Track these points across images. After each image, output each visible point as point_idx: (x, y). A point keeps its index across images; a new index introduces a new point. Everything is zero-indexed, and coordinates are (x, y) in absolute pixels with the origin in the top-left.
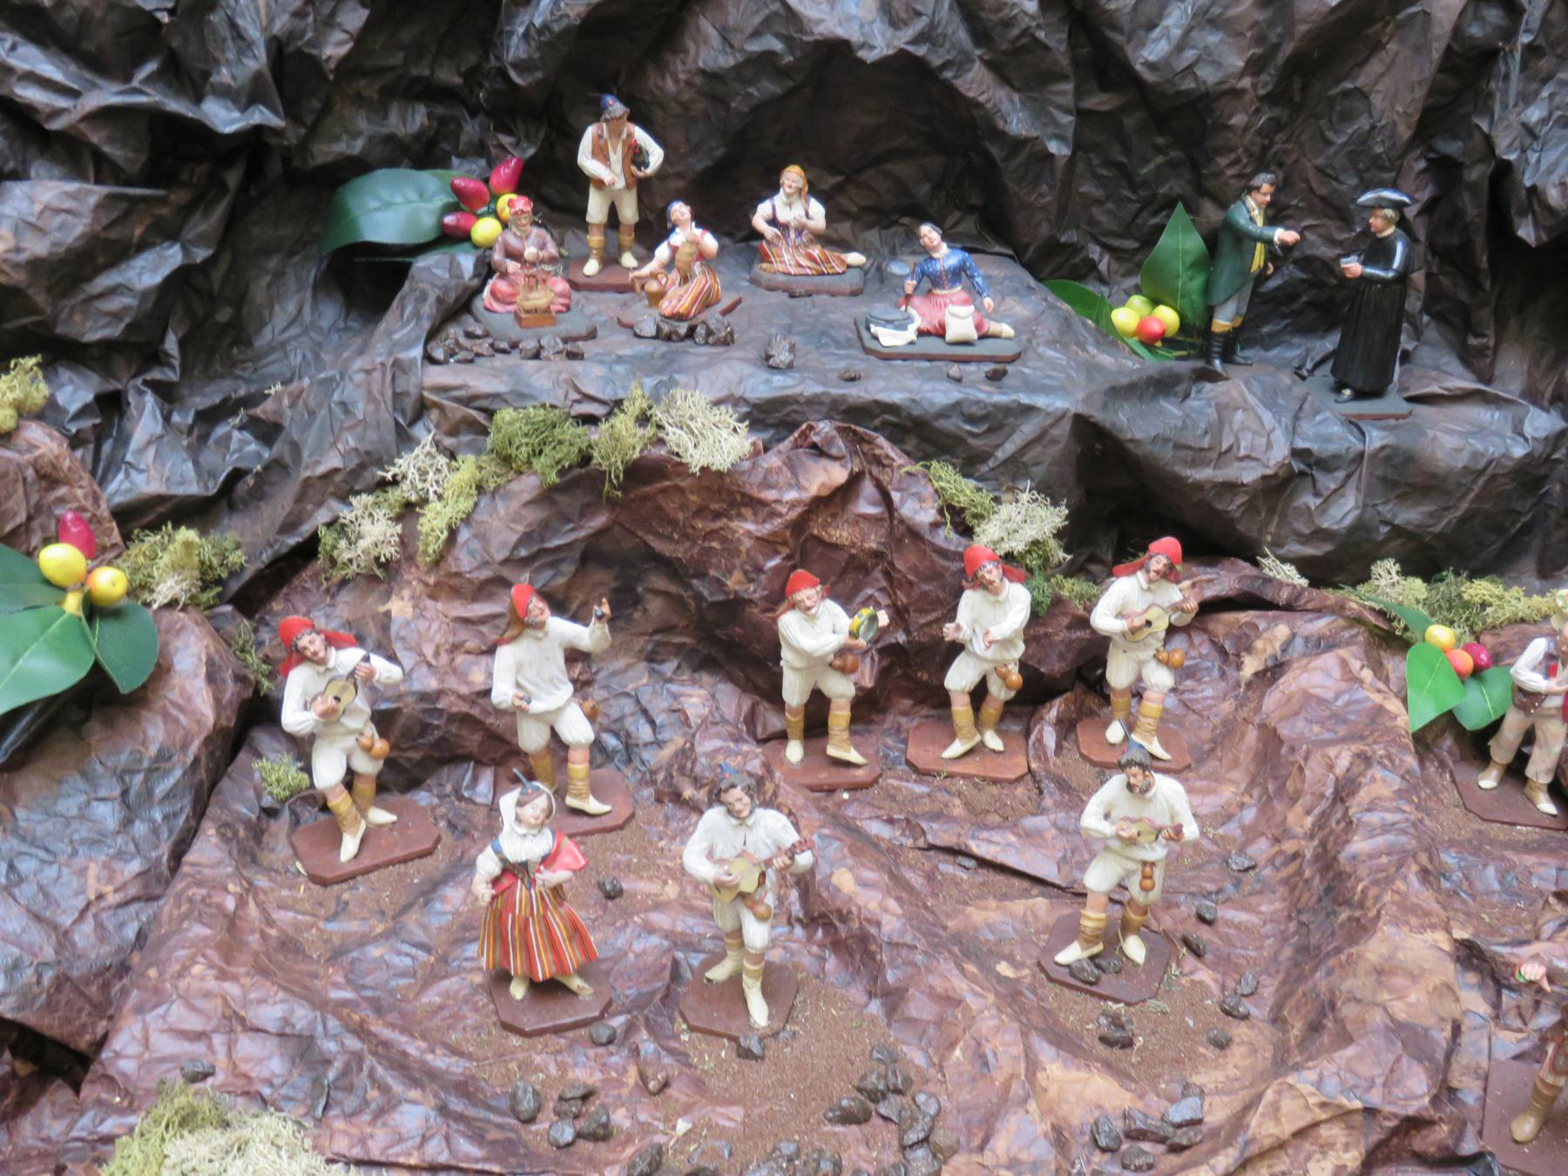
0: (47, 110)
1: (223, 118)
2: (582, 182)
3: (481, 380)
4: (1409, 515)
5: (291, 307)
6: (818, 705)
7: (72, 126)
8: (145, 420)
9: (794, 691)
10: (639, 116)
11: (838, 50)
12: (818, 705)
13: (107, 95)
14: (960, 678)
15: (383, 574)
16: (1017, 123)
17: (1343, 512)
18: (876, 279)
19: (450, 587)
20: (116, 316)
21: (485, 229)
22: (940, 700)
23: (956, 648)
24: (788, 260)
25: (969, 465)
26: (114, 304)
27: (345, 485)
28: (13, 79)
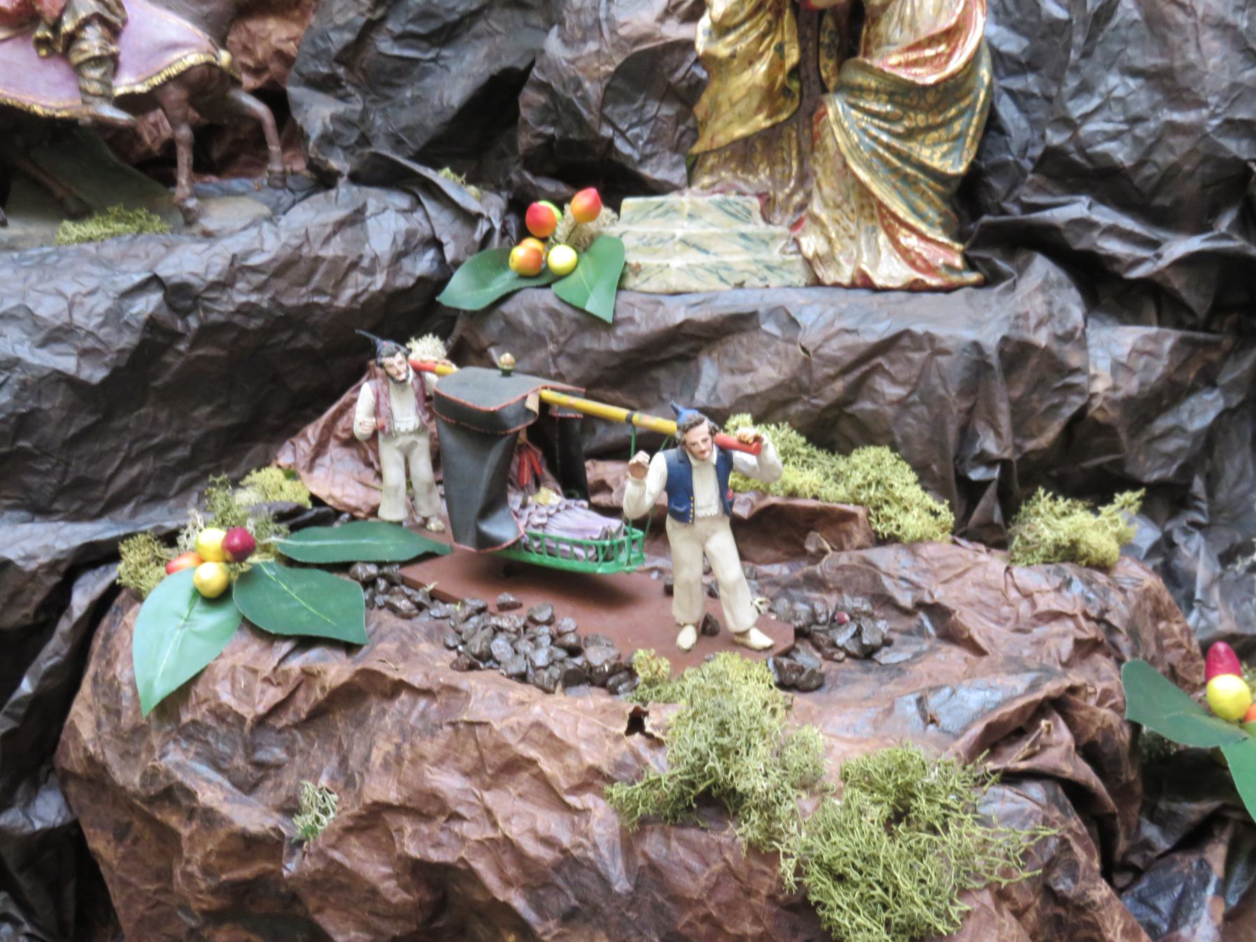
0: (1130, 260)
5: (1237, 462)
7: (1160, 272)
13: (1181, 246)
20: (1171, 457)
26: (1171, 445)
28: (1096, 234)
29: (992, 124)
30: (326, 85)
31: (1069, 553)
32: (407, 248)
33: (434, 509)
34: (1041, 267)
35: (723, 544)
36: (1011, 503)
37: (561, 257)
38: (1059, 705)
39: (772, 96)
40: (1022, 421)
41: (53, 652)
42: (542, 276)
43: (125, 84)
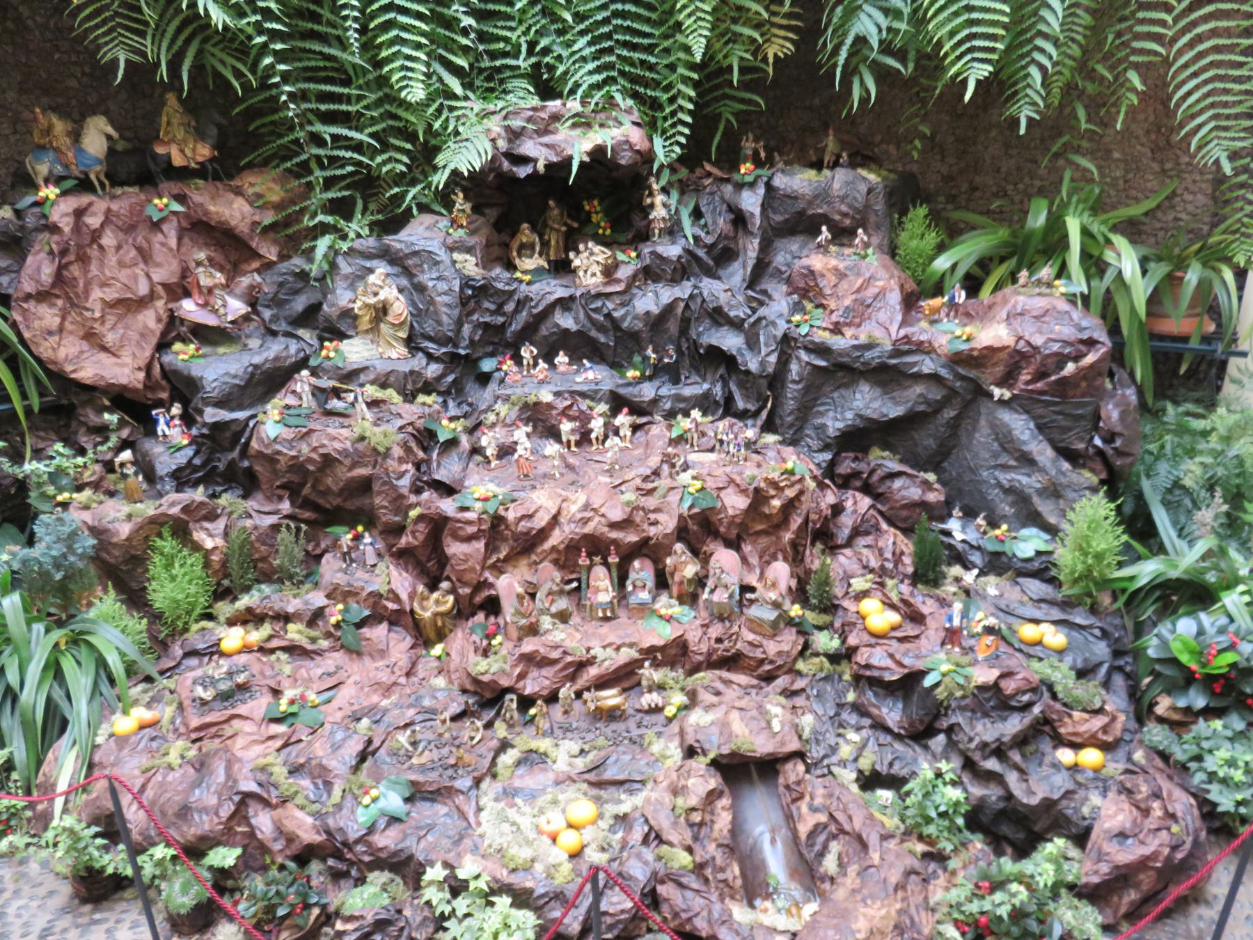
1: (463, 352)
2: (521, 358)
3: (508, 392)
4: (682, 405)
6: (569, 442)
8: (451, 404)
9: (564, 439)
10: (532, 344)
11: (567, 331)
12: (569, 442)
13: (444, 350)
14: (593, 436)
15: (494, 425)
16: (602, 339)
17: (668, 406)
18: (578, 372)
19: (506, 425)
21: (505, 367)
22: (590, 442)
23: (591, 431)
24: (562, 368)
25: (593, 399)
27: (486, 411)
29: (412, 326)
30: (268, 306)
31: (424, 404)
32: (299, 351)
33: (314, 404)
34: (420, 354)
35: (364, 406)
36: (414, 397)
37: (332, 354)
38: (411, 424)
39: (371, 322)
40: (414, 383)
41: (247, 434)
42: (328, 358)
43: (230, 318)
